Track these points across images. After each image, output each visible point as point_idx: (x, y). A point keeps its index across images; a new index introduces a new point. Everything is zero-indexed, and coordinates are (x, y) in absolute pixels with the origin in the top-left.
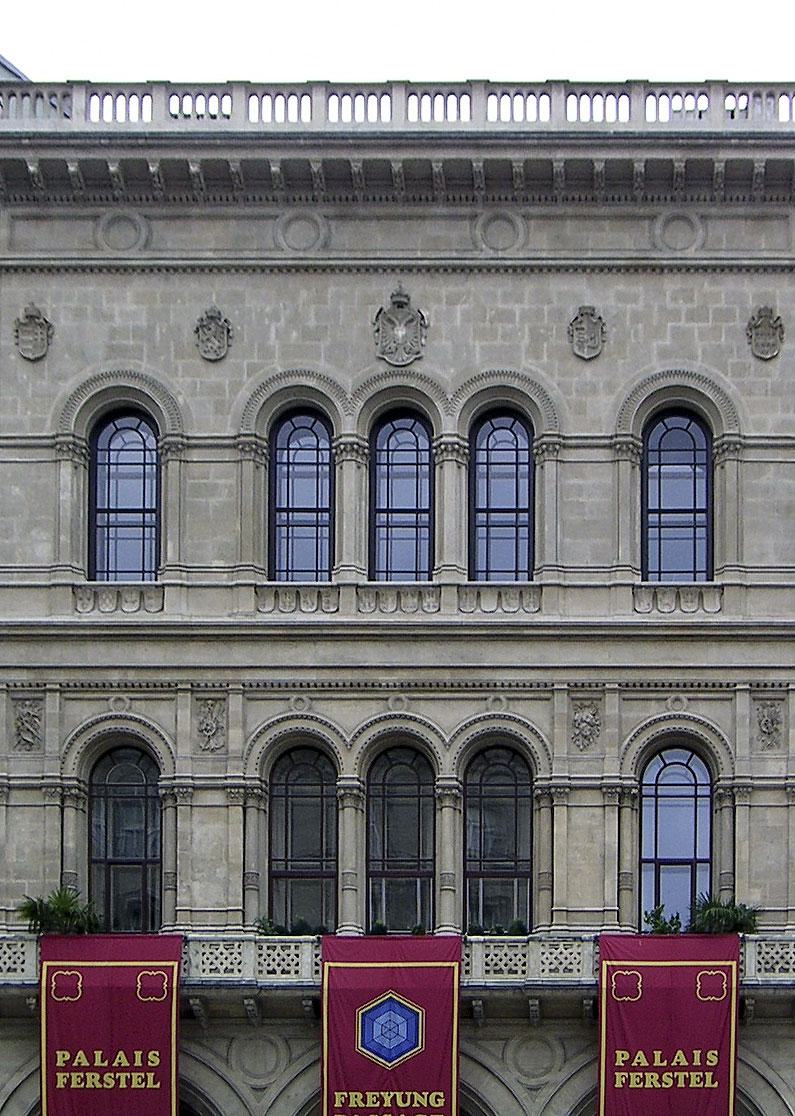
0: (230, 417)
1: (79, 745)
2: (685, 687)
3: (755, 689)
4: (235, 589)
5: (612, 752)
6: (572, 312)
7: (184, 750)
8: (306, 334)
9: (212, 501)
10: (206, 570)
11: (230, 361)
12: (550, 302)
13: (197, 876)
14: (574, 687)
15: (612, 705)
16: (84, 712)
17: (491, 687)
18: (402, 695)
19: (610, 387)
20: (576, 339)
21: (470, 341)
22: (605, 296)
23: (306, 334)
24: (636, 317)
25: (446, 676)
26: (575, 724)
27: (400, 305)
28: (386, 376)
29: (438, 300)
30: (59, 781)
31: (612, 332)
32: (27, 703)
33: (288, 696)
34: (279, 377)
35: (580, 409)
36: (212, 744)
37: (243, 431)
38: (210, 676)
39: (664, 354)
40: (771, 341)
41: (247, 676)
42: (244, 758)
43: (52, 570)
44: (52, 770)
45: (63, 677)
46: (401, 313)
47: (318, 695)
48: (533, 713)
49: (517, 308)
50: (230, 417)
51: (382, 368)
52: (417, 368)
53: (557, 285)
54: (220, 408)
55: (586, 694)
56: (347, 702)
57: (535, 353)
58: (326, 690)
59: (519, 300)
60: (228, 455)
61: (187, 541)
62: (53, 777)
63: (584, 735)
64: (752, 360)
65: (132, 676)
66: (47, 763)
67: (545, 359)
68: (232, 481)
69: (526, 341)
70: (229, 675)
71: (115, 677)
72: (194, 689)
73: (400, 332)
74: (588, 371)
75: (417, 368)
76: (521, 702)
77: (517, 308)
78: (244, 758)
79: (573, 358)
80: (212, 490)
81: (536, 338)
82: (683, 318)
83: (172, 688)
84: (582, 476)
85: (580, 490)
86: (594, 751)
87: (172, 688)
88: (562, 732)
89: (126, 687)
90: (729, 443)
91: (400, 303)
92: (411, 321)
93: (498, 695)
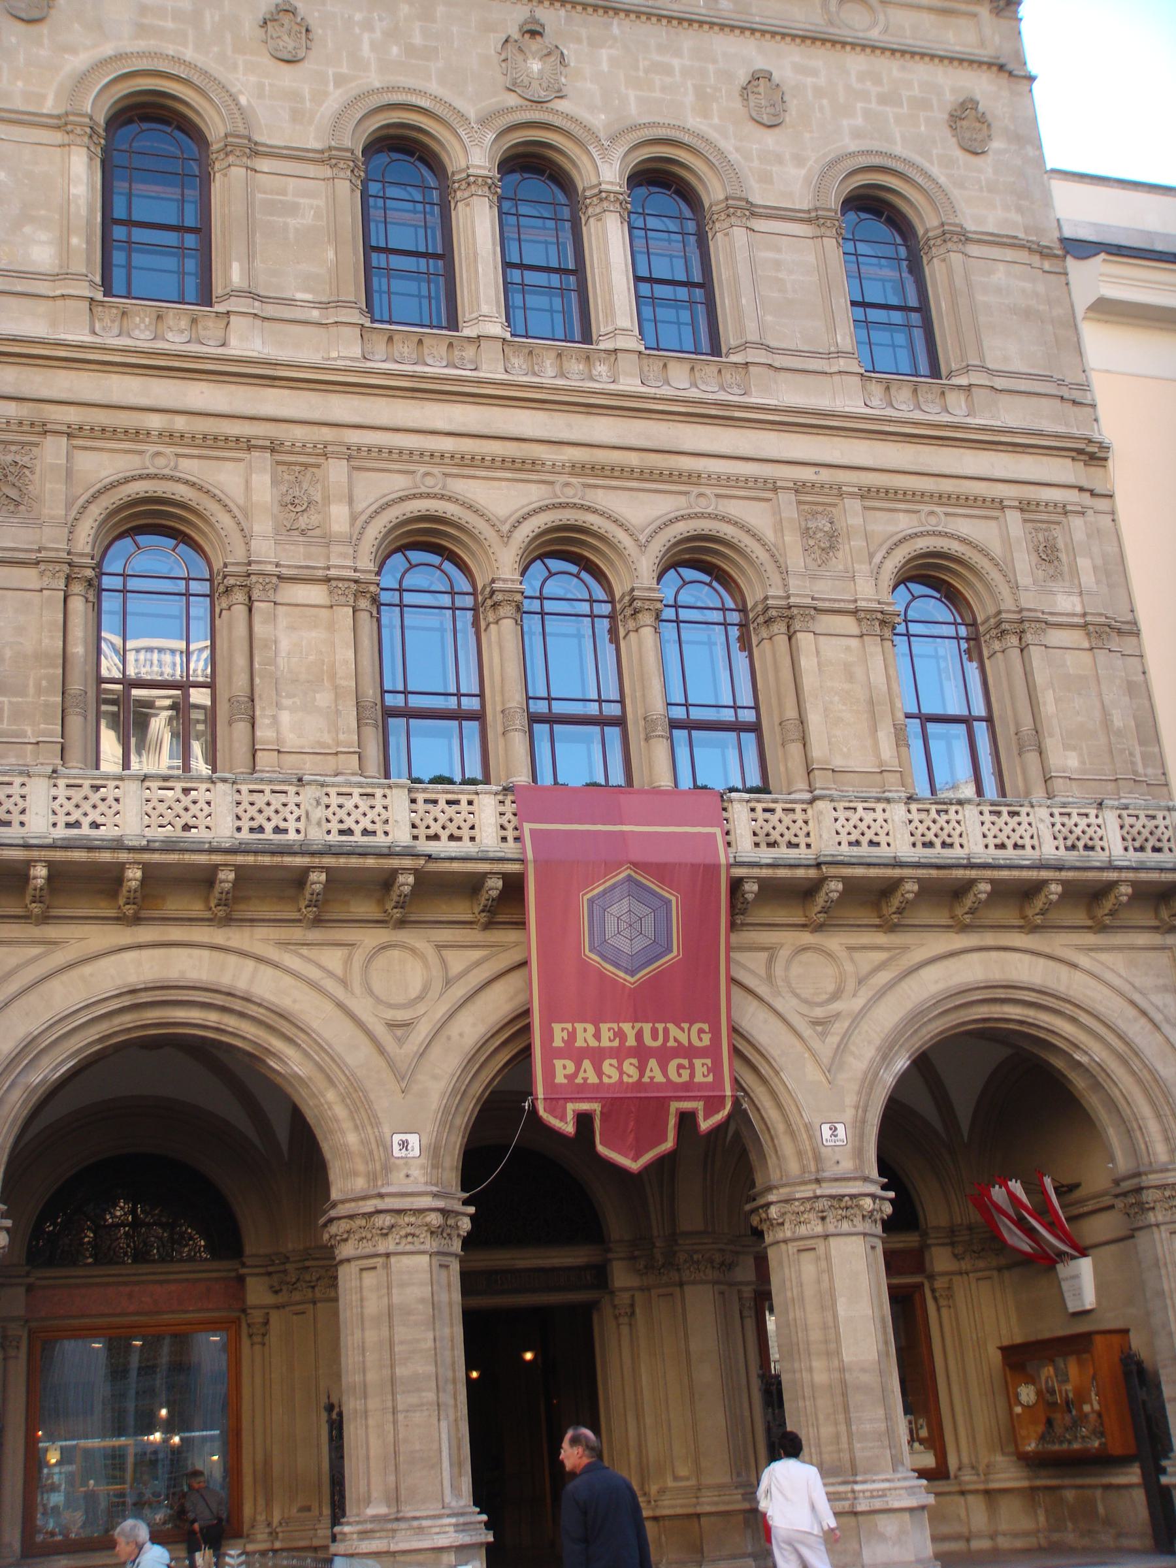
0: (312, 129)
1: (96, 511)
2: (942, 499)
3: (1025, 507)
4: (333, 329)
5: (863, 569)
6: (742, 77)
7: (262, 526)
8: (410, 50)
9: (292, 222)
10: (289, 302)
11: (305, 65)
12: (715, 61)
13: (286, 702)
14: (799, 488)
15: (852, 514)
16: (101, 466)
17: (693, 478)
18: (573, 480)
19: (799, 160)
20: (752, 104)
21: (623, 88)
22: (786, 63)
23: (410, 50)
24: (819, 92)
25: (633, 459)
26: (806, 533)
27: (534, 33)
28: (520, 108)
29: (579, 40)
30: (64, 555)
31: (793, 104)
32: (13, 448)
33: (412, 468)
34: (378, 91)
35: (766, 178)
36: (303, 522)
37: (333, 144)
38: (299, 432)
39: (857, 134)
40: (979, 137)
41: (355, 437)
42: (354, 542)
43: (55, 277)
44: (53, 539)
45: (72, 416)
46: (535, 45)
47: (455, 471)
48: (755, 515)
49: (676, 62)
50: (312, 129)
51: (512, 100)
52: (562, 105)
53: (724, 45)
54: (297, 116)
55: (815, 497)
56: (496, 484)
57: (706, 114)
58: (467, 463)
59: (678, 53)
60: (311, 170)
61: (258, 264)
62: (57, 550)
63: (825, 544)
64: (959, 154)
65: (180, 423)
66: (46, 530)
67: (716, 121)
68: (321, 203)
69: (690, 99)
70: (327, 434)
71: (155, 422)
72: (274, 447)
73: (535, 66)
74: (770, 139)
75: (562, 105)
76: (733, 501)
77: (676, 62)
78: (354, 542)
79: (751, 126)
80: (293, 209)
81: (701, 95)
82: (874, 99)
83: (249, 445)
84: (779, 250)
85: (778, 264)
86: (838, 564)
87: (249, 445)
88: (792, 542)
89: (170, 437)
90: (953, 233)
91: (534, 32)
92: (549, 54)
93: (703, 489)
